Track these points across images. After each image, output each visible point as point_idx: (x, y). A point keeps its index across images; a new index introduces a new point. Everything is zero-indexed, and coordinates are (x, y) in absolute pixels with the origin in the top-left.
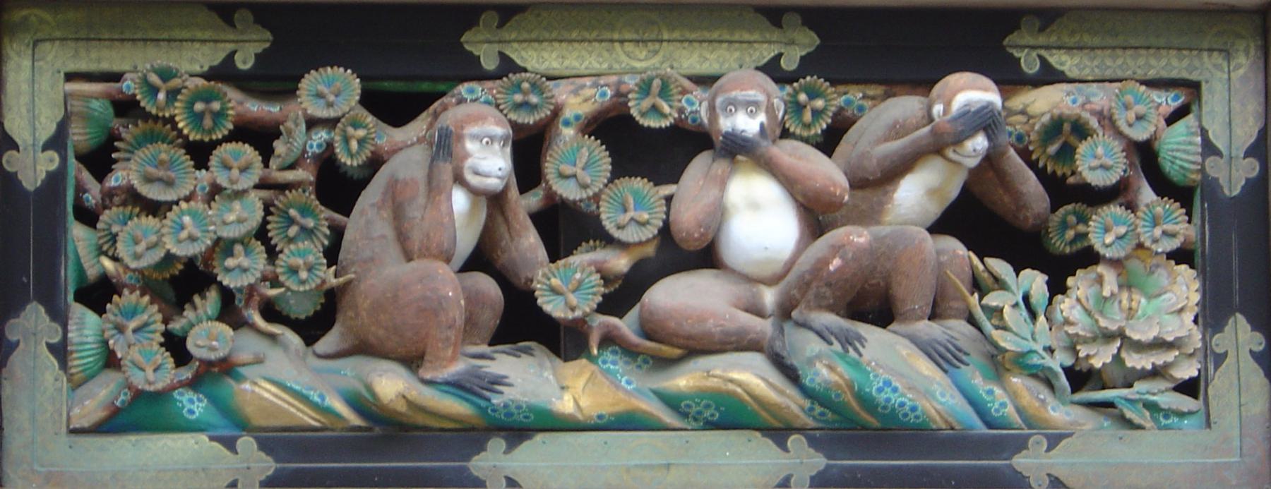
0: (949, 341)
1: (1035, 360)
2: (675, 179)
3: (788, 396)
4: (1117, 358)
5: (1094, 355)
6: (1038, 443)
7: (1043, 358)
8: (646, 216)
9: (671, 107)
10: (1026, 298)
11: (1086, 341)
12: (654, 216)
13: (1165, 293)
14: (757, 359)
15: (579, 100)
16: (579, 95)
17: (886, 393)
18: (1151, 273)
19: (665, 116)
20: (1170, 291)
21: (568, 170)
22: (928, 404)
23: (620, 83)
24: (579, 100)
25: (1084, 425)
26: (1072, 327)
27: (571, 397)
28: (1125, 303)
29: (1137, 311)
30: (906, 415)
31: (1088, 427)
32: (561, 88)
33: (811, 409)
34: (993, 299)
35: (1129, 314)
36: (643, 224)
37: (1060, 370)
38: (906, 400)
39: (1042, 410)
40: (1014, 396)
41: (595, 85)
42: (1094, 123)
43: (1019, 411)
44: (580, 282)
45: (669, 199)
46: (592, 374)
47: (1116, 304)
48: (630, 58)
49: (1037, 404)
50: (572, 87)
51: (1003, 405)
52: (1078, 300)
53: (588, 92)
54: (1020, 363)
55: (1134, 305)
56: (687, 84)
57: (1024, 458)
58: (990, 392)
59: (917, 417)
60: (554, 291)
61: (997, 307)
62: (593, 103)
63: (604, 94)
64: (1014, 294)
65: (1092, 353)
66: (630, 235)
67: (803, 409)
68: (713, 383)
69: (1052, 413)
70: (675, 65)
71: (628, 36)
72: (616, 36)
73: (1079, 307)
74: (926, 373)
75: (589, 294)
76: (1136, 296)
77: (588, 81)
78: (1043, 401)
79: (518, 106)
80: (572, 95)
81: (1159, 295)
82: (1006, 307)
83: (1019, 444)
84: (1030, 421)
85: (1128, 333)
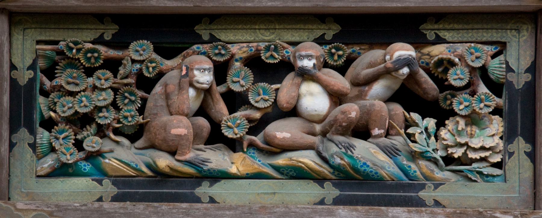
0: (392, 146)
1: (429, 155)
7: (432, 154)
9: (278, 55)
12: (271, 97)
14: (311, 153)
16: (242, 50)
19: (276, 59)
21: (235, 79)
22: (382, 171)
27: (235, 167)
30: (373, 175)
36: (266, 100)
38: (373, 170)
41: (248, 46)
44: (239, 124)
45: (277, 90)
48: (263, 35)
49: (429, 172)
53: (245, 49)
56: (286, 45)
60: (229, 127)
62: (247, 53)
63: (251, 50)
66: (261, 105)
67: (330, 172)
70: (281, 38)
74: (383, 159)
75: (243, 128)
78: (432, 171)
79: (216, 55)
82: (417, 134)
84: (427, 178)
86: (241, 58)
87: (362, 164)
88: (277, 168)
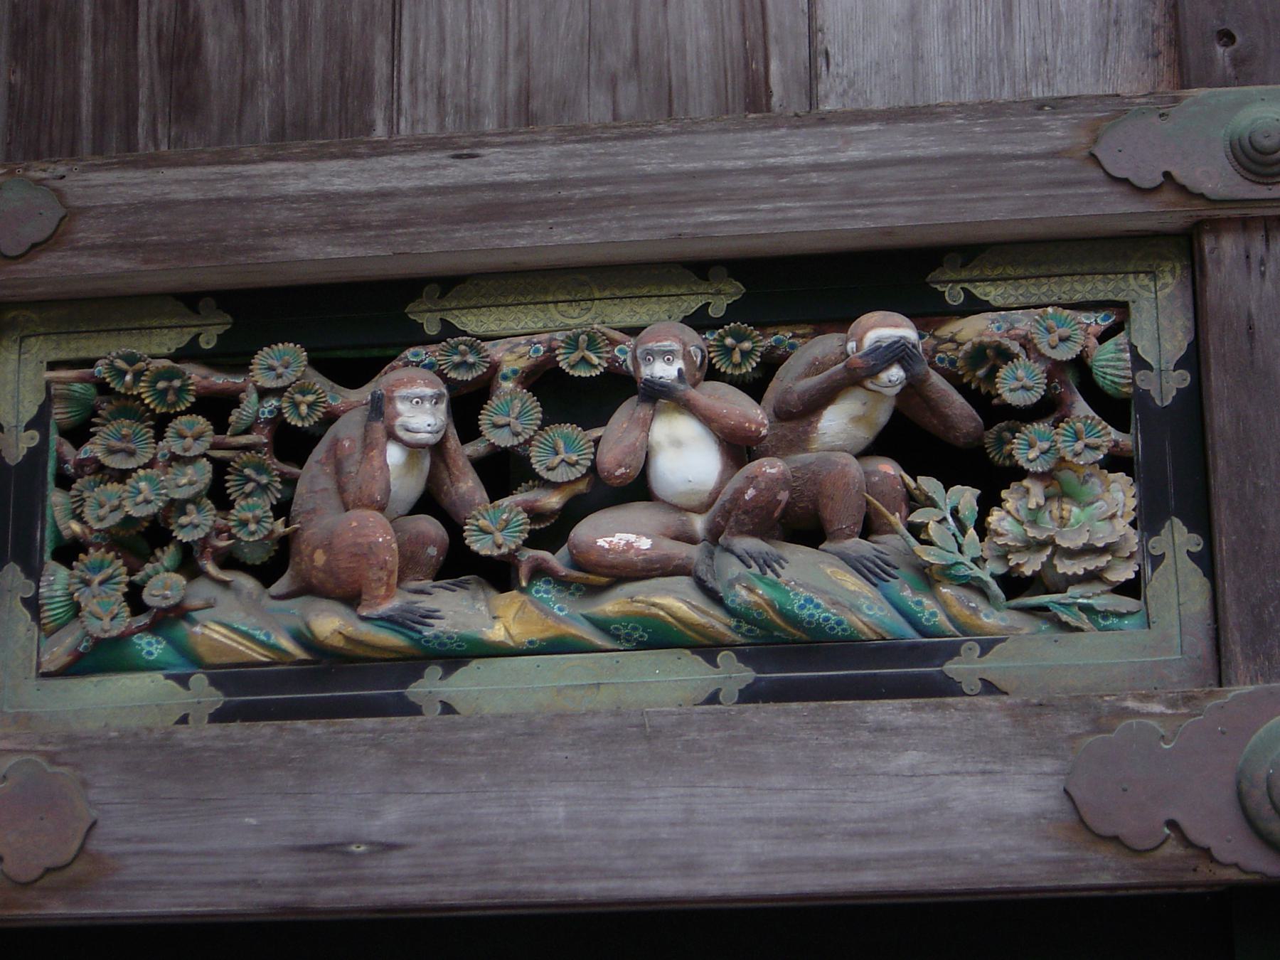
2: (603, 422)
3: (711, 616)
4: (1049, 564)
5: (1023, 564)
6: (970, 649)
7: (971, 569)
8: (575, 458)
10: (955, 512)
11: (1018, 550)
13: (1097, 501)
15: (514, 356)
16: (514, 352)
17: (809, 609)
18: (1085, 482)
19: (595, 367)
20: (1101, 499)
23: (552, 339)
24: (514, 356)
25: (1021, 629)
26: (1001, 538)
28: (1056, 513)
29: (1069, 520)
30: (832, 629)
31: (1026, 630)
32: (498, 347)
33: (738, 627)
34: (917, 517)
35: (1062, 522)
37: (989, 579)
39: (974, 617)
40: (944, 605)
41: (529, 343)
42: (1015, 347)
43: (952, 619)
44: (507, 522)
46: (522, 605)
47: (1047, 513)
50: (508, 346)
51: (933, 614)
52: (1008, 512)
53: (522, 350)
54: (947, 574)
55: (1065, 514)
57: (955, 664)
58: (919, 603)
59: (844, 630)
60: (483, 531)
61: (922, 522)
63: (537, 351)
64: (940, 509)
65: (1021, 562)
66: (559, 476)
68: (639, 607)
69: (985, 620)
70: (606, 320)
71: (562, 298)
72: (550, 298)
73: (1010, 519)
75: (516, 532)
76: (1066, 506)
77: (522, 340)
80: (508, 353)
81: (1092, 503)
82: (931, 522)
83: (952, 651)
85: (1058, 541)
86: (515, 372)
87: (802, 602)
88: (602, 625)
